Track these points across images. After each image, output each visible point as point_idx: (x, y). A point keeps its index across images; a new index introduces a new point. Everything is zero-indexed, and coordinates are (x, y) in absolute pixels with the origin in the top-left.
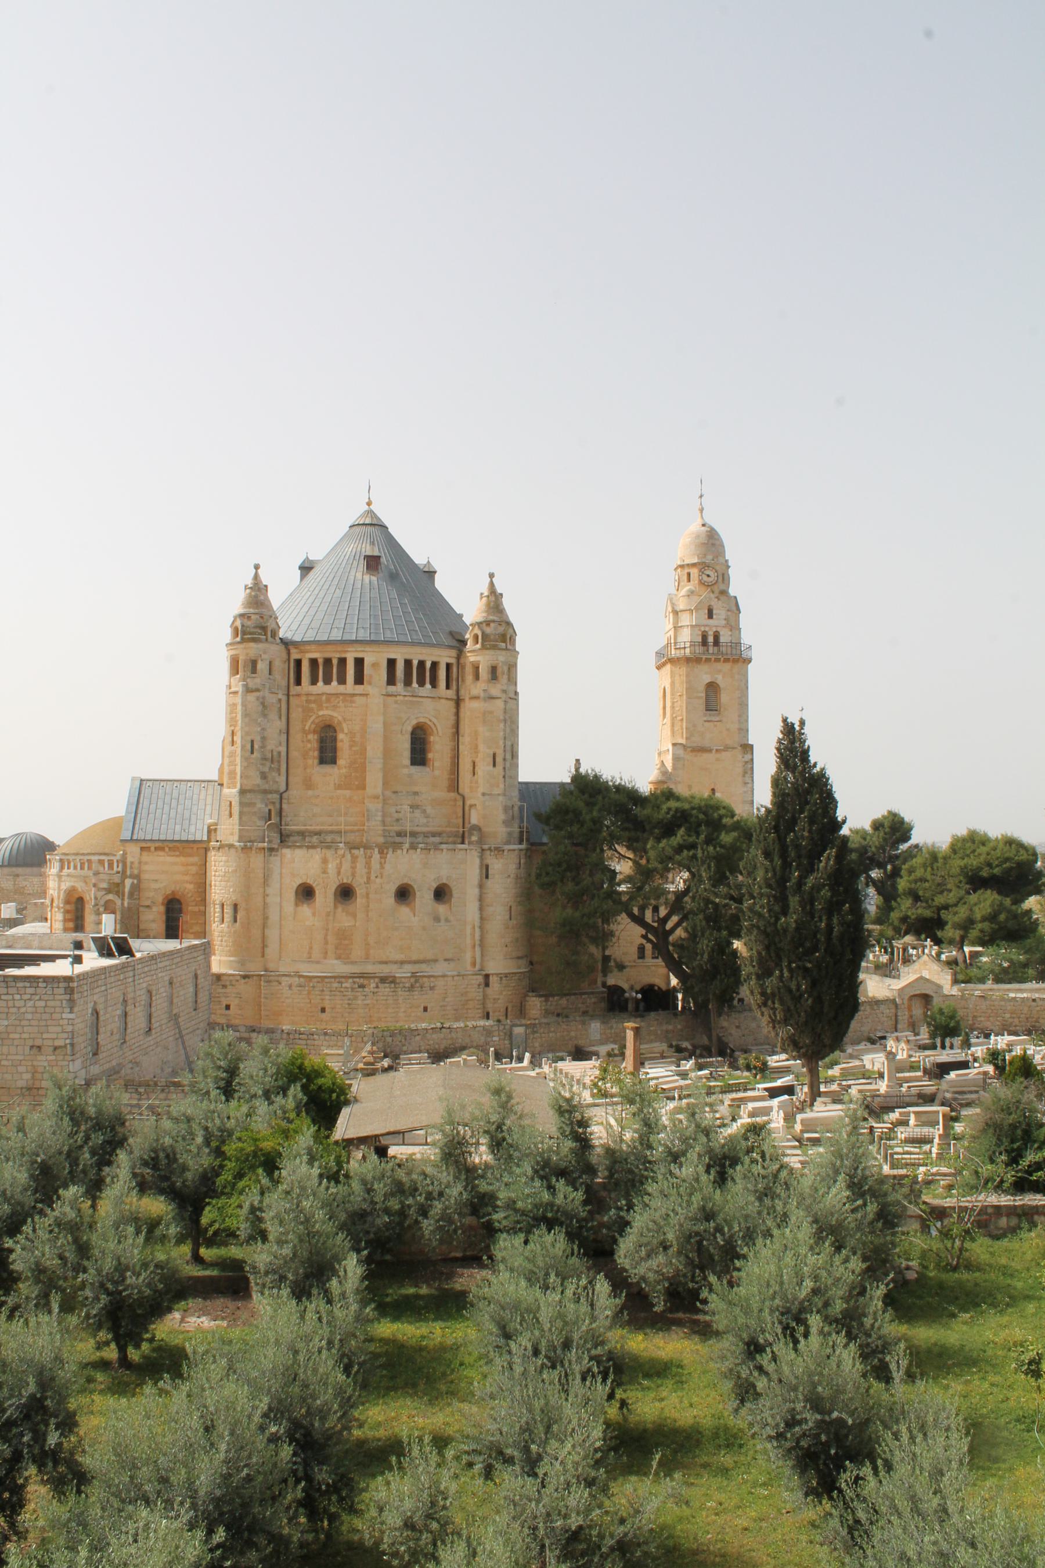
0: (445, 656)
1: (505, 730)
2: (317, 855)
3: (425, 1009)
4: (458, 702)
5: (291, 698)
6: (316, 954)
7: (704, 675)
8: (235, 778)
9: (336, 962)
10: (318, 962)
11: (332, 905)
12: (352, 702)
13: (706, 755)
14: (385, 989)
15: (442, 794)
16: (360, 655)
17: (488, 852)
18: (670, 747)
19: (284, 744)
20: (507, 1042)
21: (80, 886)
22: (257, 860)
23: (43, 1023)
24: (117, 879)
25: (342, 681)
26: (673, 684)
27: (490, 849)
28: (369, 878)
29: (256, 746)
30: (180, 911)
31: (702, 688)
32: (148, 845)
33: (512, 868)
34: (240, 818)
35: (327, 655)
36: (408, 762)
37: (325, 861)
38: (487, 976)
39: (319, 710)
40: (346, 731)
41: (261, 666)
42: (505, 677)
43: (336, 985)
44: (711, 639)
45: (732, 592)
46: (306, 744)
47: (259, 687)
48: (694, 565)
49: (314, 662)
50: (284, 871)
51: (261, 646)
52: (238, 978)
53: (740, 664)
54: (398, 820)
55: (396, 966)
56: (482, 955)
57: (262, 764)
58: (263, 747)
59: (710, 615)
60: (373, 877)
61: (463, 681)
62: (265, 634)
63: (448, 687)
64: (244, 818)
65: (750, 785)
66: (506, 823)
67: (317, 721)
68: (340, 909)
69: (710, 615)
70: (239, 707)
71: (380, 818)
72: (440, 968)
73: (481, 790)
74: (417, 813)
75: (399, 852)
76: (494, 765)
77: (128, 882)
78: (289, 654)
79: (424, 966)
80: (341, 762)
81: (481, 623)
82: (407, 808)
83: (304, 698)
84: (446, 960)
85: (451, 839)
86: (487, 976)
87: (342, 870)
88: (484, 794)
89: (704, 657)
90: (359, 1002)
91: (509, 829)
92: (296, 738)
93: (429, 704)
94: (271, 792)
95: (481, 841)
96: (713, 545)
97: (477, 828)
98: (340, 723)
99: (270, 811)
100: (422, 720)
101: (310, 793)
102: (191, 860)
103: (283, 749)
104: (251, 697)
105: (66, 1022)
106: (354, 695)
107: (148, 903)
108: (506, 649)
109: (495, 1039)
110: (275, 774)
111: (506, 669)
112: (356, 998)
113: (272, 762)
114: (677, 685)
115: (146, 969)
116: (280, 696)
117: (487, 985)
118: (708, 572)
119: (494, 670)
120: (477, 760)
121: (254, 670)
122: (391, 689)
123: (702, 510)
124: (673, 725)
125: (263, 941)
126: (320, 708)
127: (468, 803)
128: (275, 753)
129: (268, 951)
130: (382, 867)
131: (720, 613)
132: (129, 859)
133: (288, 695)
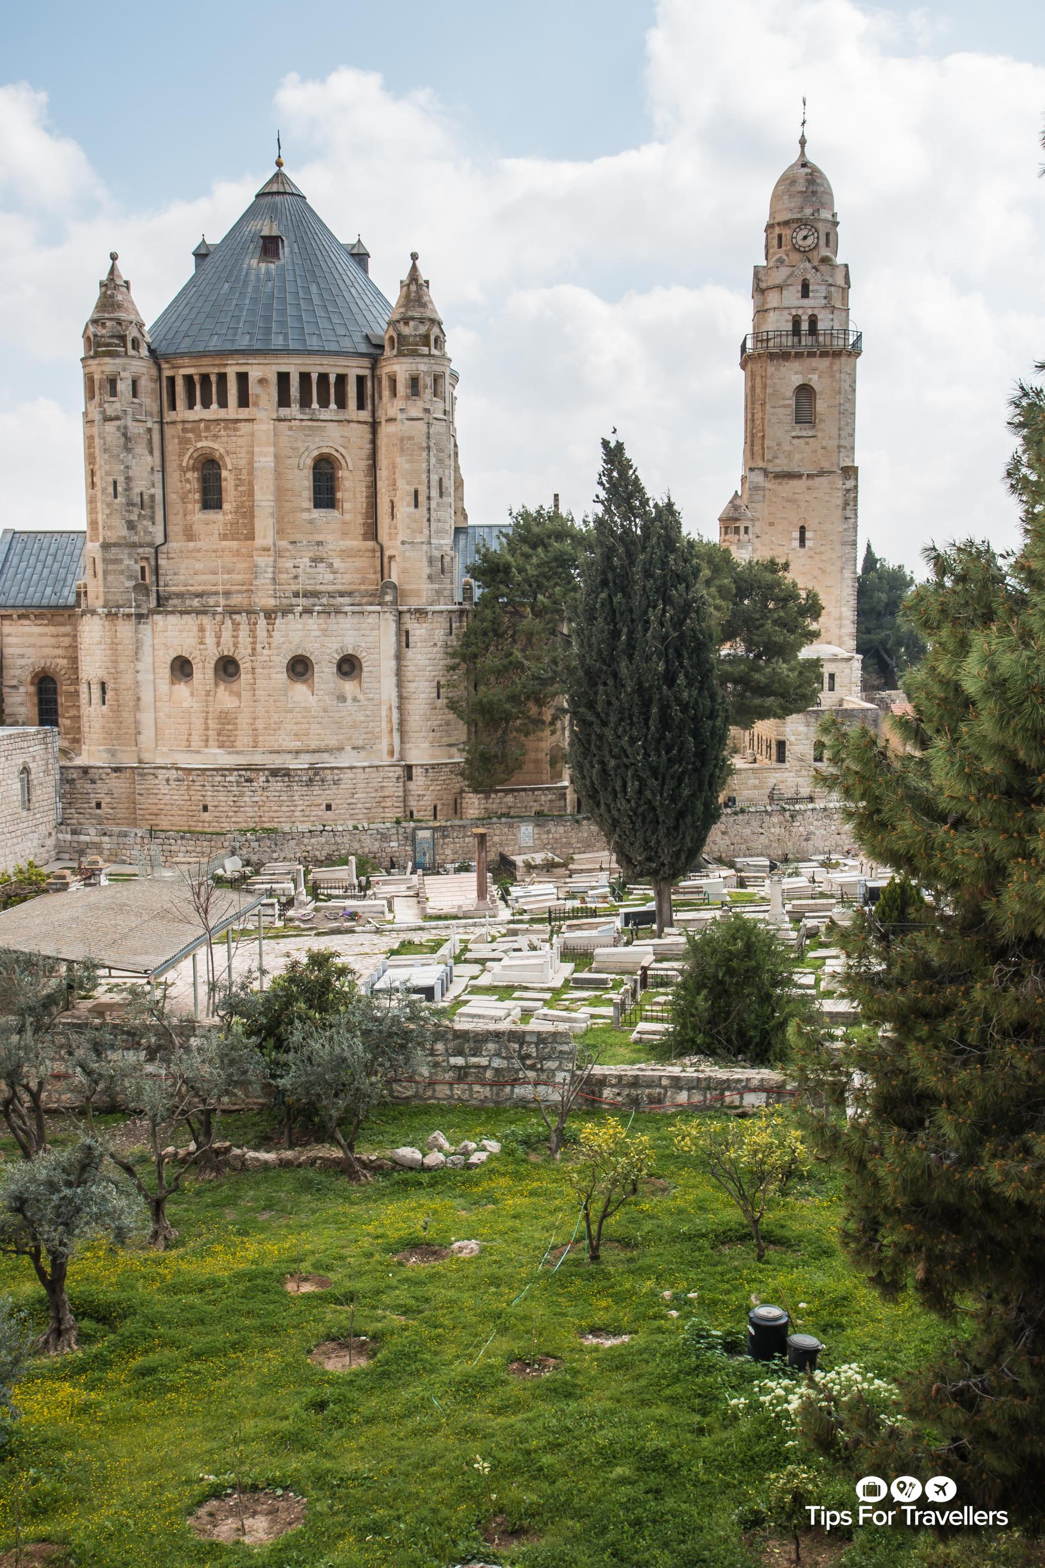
0: (354, 369)
4: (374, 426)
5: (166, 427)
6: (196, 743)
10: (198, 752)
11: (212, 681)
12: (235, 430)
13: (794, 483)
14: (277, 785)
15: (356, 543)
17: (408, 615)
22: (125, 629)
25: (223, 404)
28: (254, 649)
29: (120, 489)
31: (789, 392)
32: (9, 612)
33: (440, 634)
34: (105, 579)
37: (202, 629)
38: (409, 768)
40: (230, 467)
41: (123, 387)
43: (219, 778)
44: (805, 326)
45: (839, 260)
47: (120, 414)
49: (189, 379)
50: (156, 641)
51: (118, 361)
53: (843, 359)
56: (402, 742)
58: (128, 489)
59: (805, 292)
60: (259, 647)
61: (381, 398)
62: (125, 346)
64: (110, 578)
67: (195, 455)
68: (222, 687)
69: (805, 292)
71: (270, 575)
72: (345, 760)
73: (401, 537)
75: (291, 616)
76: (416, 506)
78: (160, 370)
79: (326, 755)
80: (226, 506)
82: (306, 560)
83: (180, 426)
85: (365, 600)
86: (409, 768)
88: (403, 543)
89: (793, 351)
90: (247, 799)
92: (174, 477)
96: (814, 193)
98: (222, 457)
99: (143, 568)
100: (325, 450)
101: (191, 544)
102: (62, 630)
103: (158, 492)
104: (110, 427)
106: (237, 421)
107: (14, 682)
108: (430, 355)
109: (392, 844)
110: (147, 523)
111: (429, 381)
112: (242, 795)
117: (410, 778)
119: (414, 382)
120: (395, 500)
121: (114, 393)
122: (284, 412)
125: (136, 728)
126: (199, 438)
127: (387, 553)
128: (146, 497)
129: (142, 738)
131: (818, 290)
133: (161, 423)
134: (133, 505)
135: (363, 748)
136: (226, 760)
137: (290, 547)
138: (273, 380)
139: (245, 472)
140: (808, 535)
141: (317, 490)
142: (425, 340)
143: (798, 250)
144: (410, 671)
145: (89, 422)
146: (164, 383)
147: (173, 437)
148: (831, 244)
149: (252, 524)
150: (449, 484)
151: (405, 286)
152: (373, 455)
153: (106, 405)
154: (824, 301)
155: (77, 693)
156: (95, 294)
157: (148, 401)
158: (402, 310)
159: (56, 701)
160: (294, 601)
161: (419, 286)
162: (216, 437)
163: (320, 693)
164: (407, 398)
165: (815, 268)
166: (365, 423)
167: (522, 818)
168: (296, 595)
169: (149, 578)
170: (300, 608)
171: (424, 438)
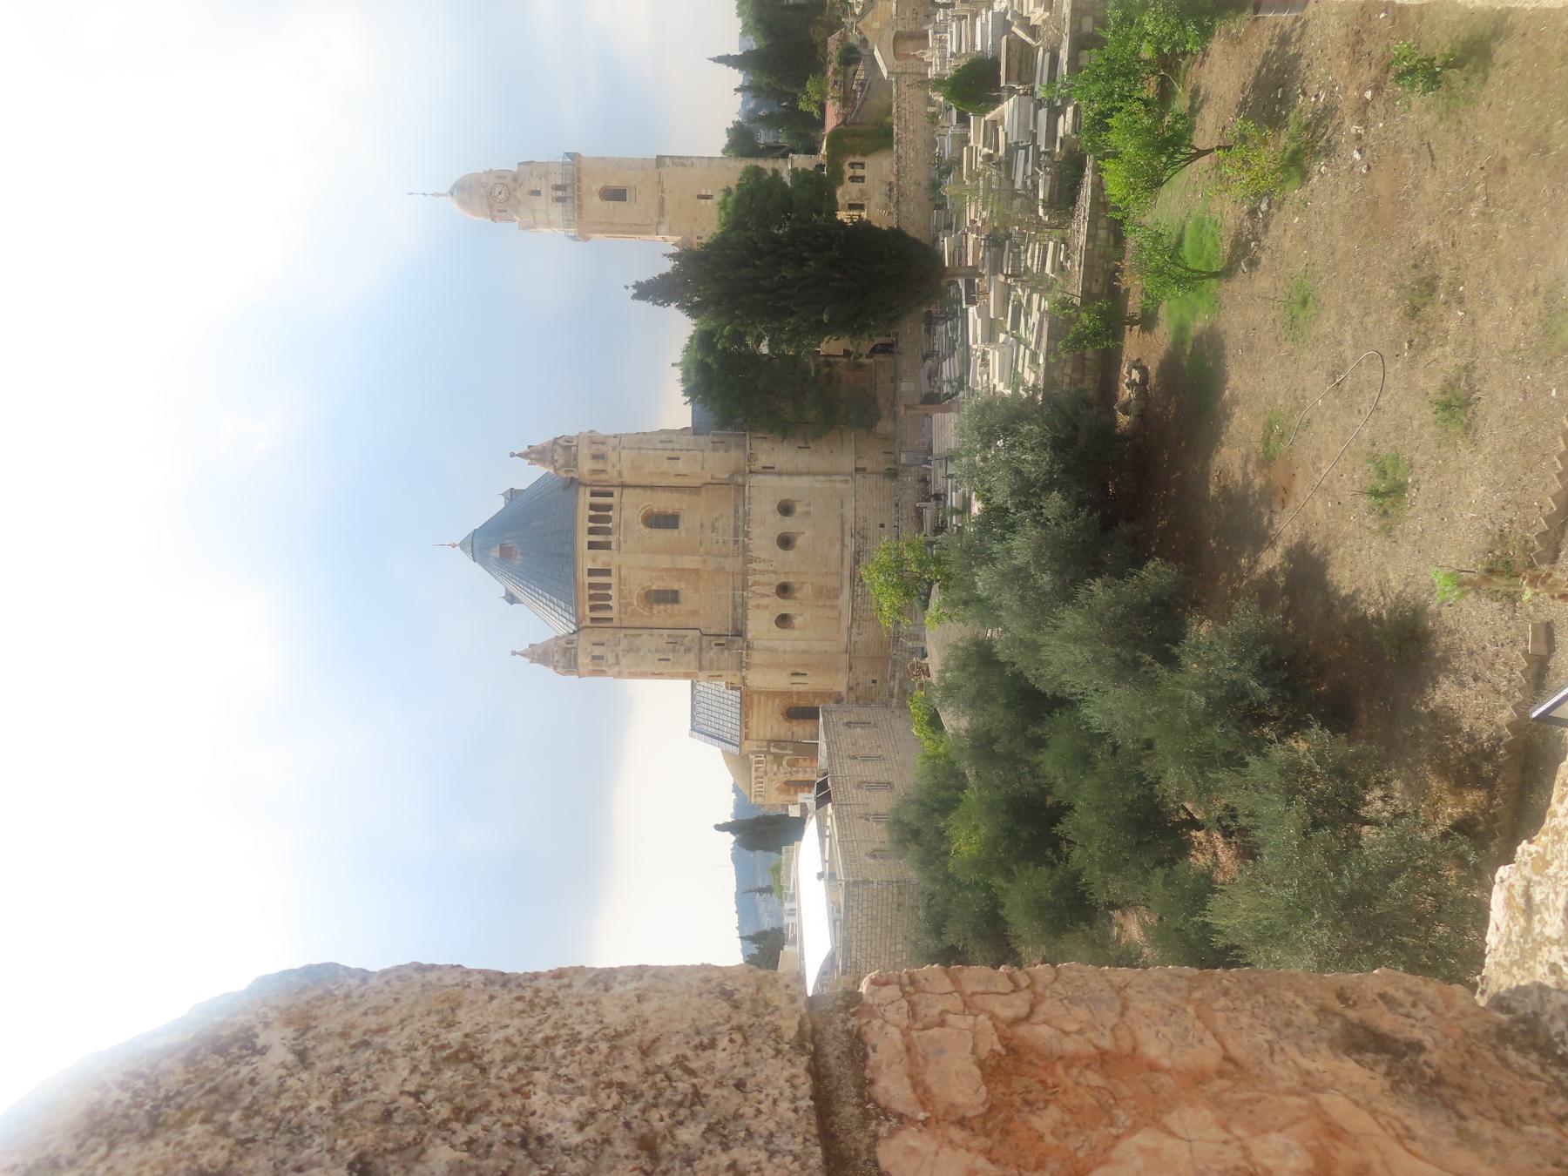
0: (585, 498)
2: (751, 614)
3: (882, 526)
4: (624, 486)
6: (834, 614)
9: (840, 600)
10: (840, 613)
13: (666, 202)
16: (586, 573)
20: (913, 469)
21: (775, 785)
22: (756, 658)
23: (880, 903)
24: (770, 758)
25: (608, 586)
27: (749, 466)
28: (773, 572)
29: (664, 657)
30: (796, 708)
33: (765, 445)
34: (723, 669)
37: (758, 606)
41: (598, 651)
42: (601, 447)
45: (515, 169)
49: (592, 608)
51: (579, 653)
55: (846, 551)
56: (838, 474)
60: (772, 569)
61: (605, 481)
62: (571, 649)
65: (694, 161)
68: (797, 595)
69: (536, 193)
71: (723, 559)
72: (849, 512)
73: (699, 470)
74: (719, 525)
75: (751, 546)
76: (678, 459)
77: (773, 750)
79: (846, 527)
80: (676, 588)
84: (842, 506)
86: (857, 470)
87: (766, 593)
88: (702, 469)
91: (733, 447)
94: (701, 645)
95: (741, 472)
97: (733, 475)
99: (716, 645)
100: (640, 520)
102: (756, 701)
103: (666, 632)
104: (623, 661)
105: (880, 887)
106: (620, 578)
108: (577, 446)
110: (686, 640)
111: (594, 447)
115: (841, 789)
118: (497, 193)
119: (595, 457)
121: (601, 658)
122: (614, 546)
123: (437, 195)
126: (631, 604)
127: (710, 480)
128: (669, 641)
131: (534, 183)
132: (755, 749)
134: (674, 648)
136: (846, 594)
138: (593, 552)
139: (654, 574)
140: (703, 193)
141: (666, 526)
142: (567, 449)
145: (620, 675)
146: (593, 625)
149: (688, 570)
150: (663, 437)
151: (534, 461)
152: (643, 487)
153: (609, 663)
155: (798, 693)
156: (537, 666)
157: (606, 636)
159: (804, 708)
160: (740, 543)
161: (532, 452)
162: (630, 592)
164: (606, 462)
167: (895, 389)
168: (736, 542)
169: (722, 641)
170: (746, 540)
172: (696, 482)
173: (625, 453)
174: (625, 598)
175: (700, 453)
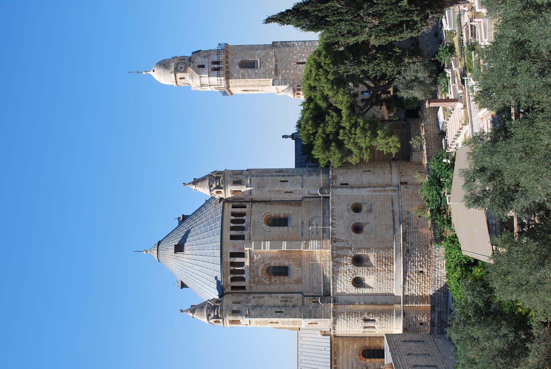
0: (229, 209)
1: (268, 176)
4: (253, 201)
5: (252, 291)
7: (235, 69)
8: (296, 321)
17: (334, 184)
18: (275, 87)
19: (277, 294)
26: (240, 86)
29: (279, 310)
34: (318, 318)
35: (229, 272)
36: (286, 228)
38: (401, 183)
39: (259, 276)
40: (269, 261)
41: (235, 307)
42: (239, 176)
44: (216, 66)
45: (190, 55)
46: (277, 284)
48: (175, 76)
49: (233, 280)
52: (405, 318)
54: (317, 233)
56: (390, 186)
57: (288, 306)
58: (279, 307)
59: (203, 66)
60: (349, 246)
61: (242, 199)
62: (218, 306)
63: (245, 207)
66: (318, 175)
69: (203, 66)
70: (258, 319)
73: (300, 188)
76: (287, 181)
78: (228, 293)
79: (397, 218)
80: (286, 264)
81: (210, 189)
84: (393, 206)
85: (327, 204)
88: (302, 187)
92: (273, 288)
93: (255, 217)
99: (313, 302)
100: (263, 221)
101: (303, 280)
103: (280, 295)
113: (287, 301)
114: (241, 84)
116: (251, 297)
117: (406, 183)
122: (246, 238)
124: (263, 86)
127: (307, 195)
128: (282, 300)
130: (342, 241)
133: (251, 293)
135: (392, 202)
137: (305, 235)
138: (233, 241)
143: (186, 70)
144: (358, 183)
147: (257, 288)
148: (184, 58)
153: (243, 314)
154: (206, 58)
158: (205, 188)
163: (368, 220)
165: (193, 63)
166: (252, 205)
171: (258, 178)
172: (298, 197)
173: (254, 179)
174: (253, 271)
175: (300, 178)
